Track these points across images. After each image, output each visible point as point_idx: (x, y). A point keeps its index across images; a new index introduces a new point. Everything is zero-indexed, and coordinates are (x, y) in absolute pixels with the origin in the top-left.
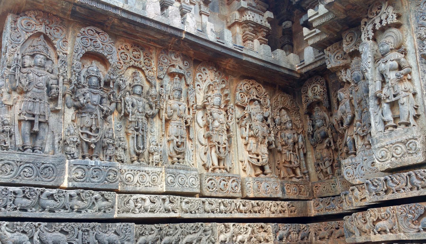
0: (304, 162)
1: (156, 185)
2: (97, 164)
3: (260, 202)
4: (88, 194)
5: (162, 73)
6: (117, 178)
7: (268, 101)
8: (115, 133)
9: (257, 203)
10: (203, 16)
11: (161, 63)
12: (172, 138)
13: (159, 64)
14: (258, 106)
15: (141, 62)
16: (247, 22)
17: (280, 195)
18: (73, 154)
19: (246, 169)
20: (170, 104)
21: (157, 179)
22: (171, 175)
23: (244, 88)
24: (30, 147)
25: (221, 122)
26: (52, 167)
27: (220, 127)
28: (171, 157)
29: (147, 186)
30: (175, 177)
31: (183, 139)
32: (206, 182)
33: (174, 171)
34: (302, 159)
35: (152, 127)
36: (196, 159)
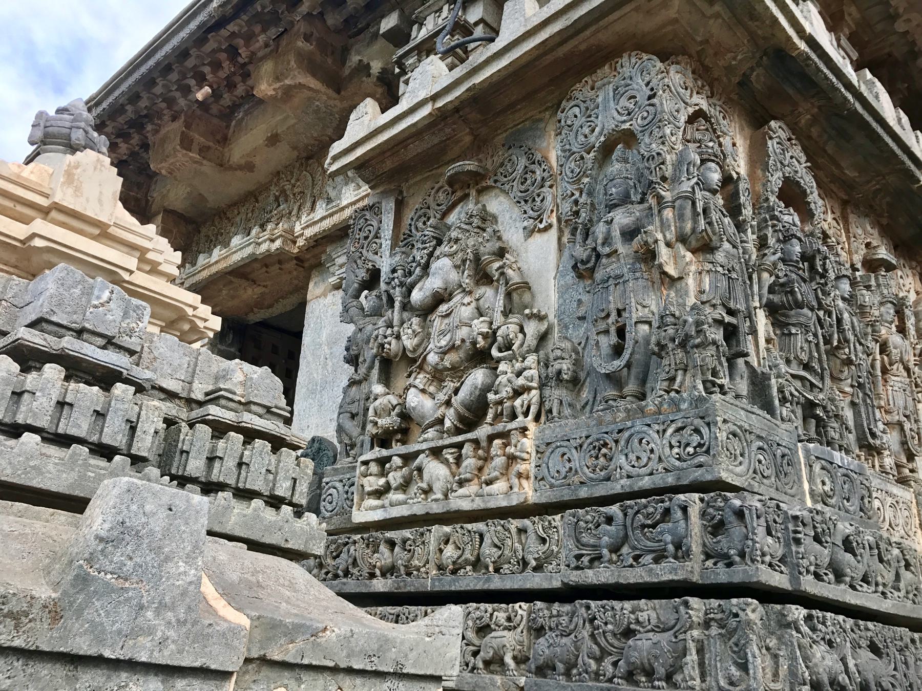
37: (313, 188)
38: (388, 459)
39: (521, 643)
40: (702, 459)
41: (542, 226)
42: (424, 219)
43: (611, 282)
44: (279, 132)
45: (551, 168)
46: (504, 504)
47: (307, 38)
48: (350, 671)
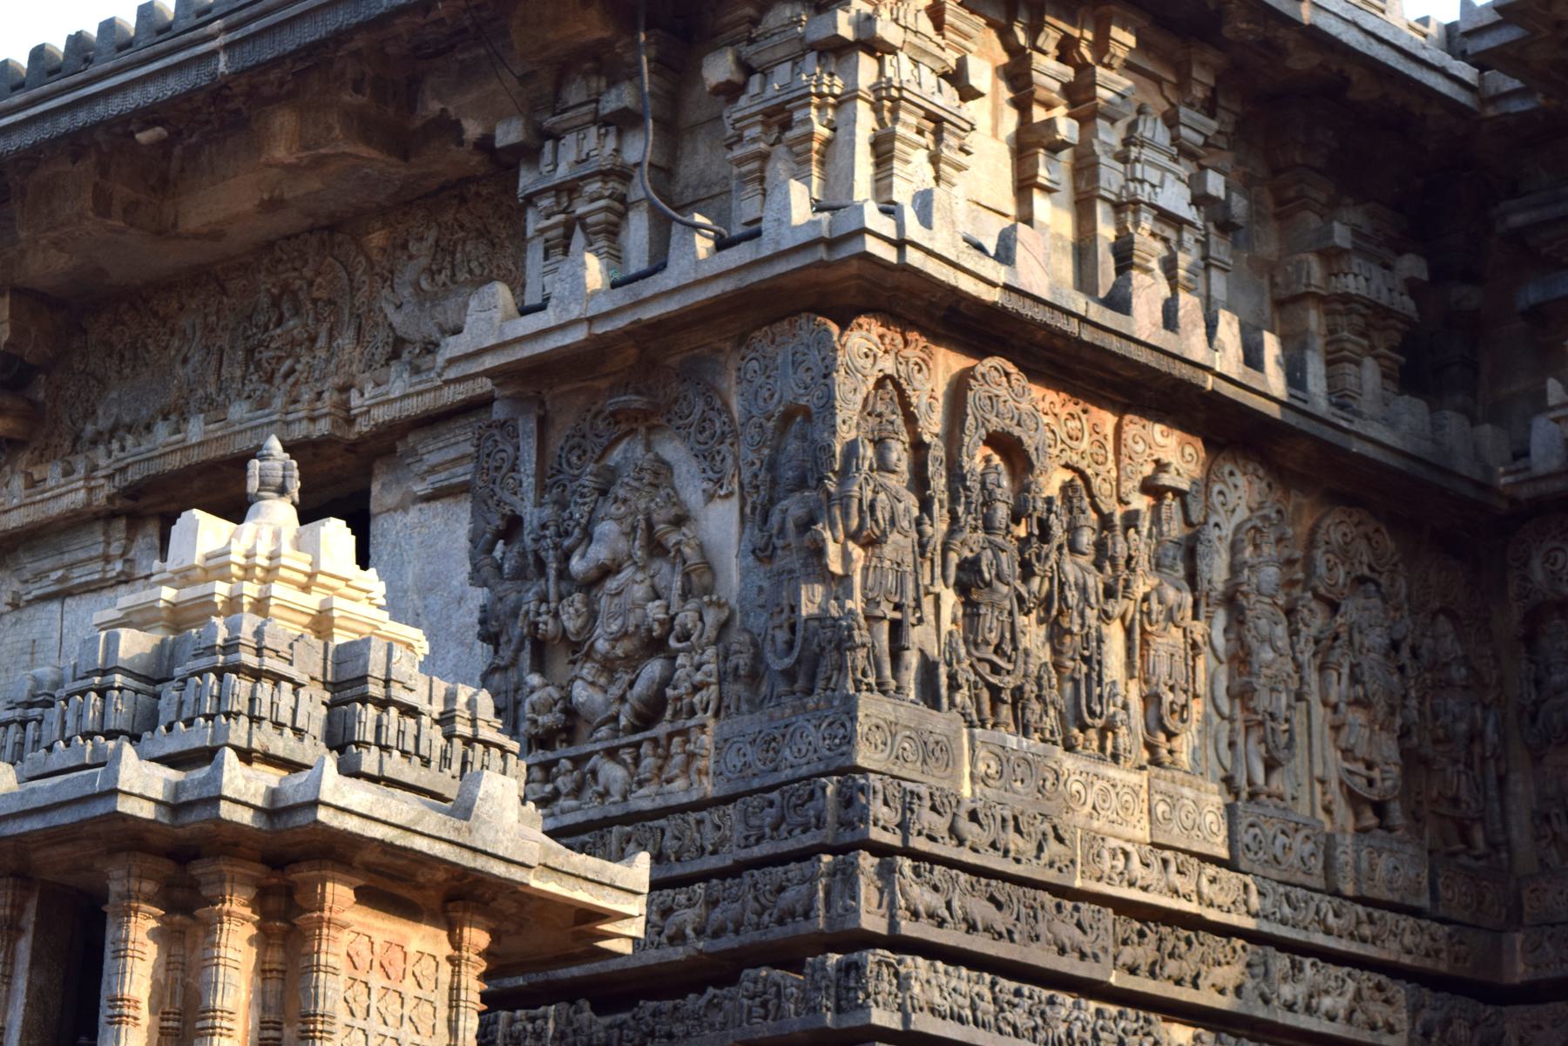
0: (1496, 806)
3: (1376, 914)
7: (1401, 584)
9: (1369, 915)
10: (1214, 273)
14: (1376, 601)
16: (1346, 298)
17: (1424, 902)
19: (1334, 807)
23: (1336, 537)
34: (1493, 793)
37: (353, 297)
38: (555, 762)
39: (699, 916)
40: (844, 748)
41: (722, 493)
42: (578, 452)
43: (785, 576)
44: (286, 196)
45: (732, 420)
46: (685, 800)
47: (357, 89)
48: (586, 879)
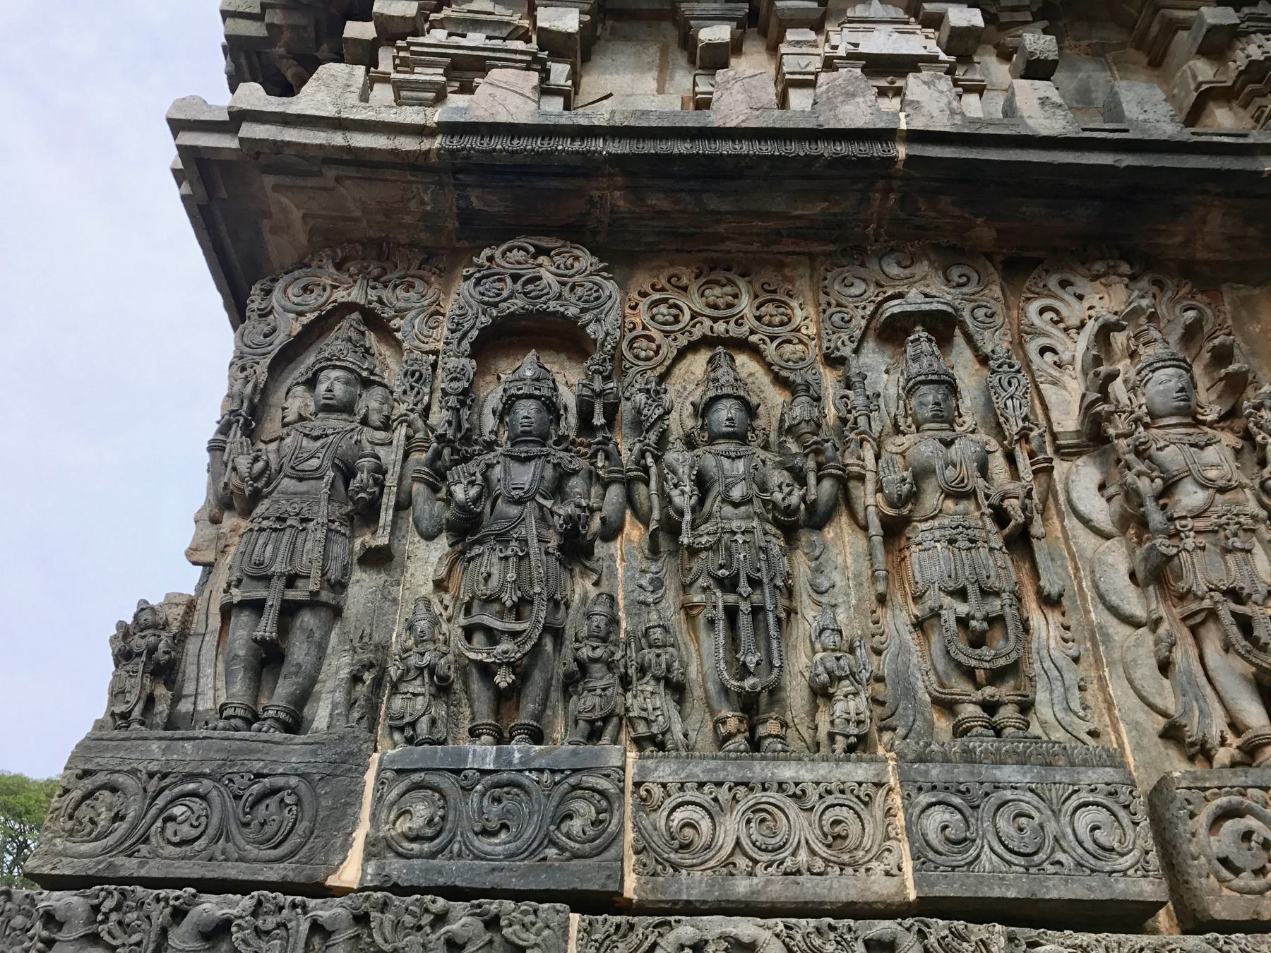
1: (855, 865)
2: (510, 763)
4: (413, 914)
5: (845, 338)
6: (612, 828)
8: (628, 614)
11: (833, 302)
12: (929, 603)
13: (824, 306)
15: (742, 318)
18: (413, 725)
20: (899, 450)
21: (854, 828)
22: (942, 796)
24: (240, 712)
25: (1221, 483)
26: (294, 791)
27: (1219, 509)
28: (947, 706)
29: (798, 872)
30: (968, 812)
31: (997, 603)
32: (1202, 832)
33: (961, 773)
35: (818, 570)
36: (1110, 705)
